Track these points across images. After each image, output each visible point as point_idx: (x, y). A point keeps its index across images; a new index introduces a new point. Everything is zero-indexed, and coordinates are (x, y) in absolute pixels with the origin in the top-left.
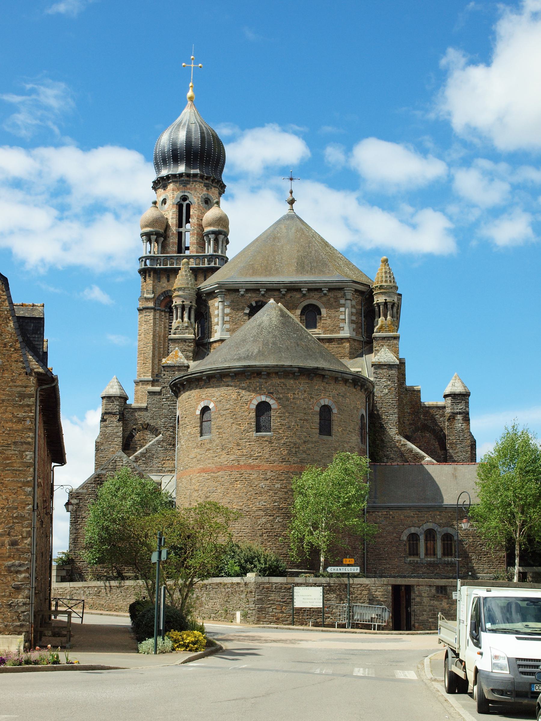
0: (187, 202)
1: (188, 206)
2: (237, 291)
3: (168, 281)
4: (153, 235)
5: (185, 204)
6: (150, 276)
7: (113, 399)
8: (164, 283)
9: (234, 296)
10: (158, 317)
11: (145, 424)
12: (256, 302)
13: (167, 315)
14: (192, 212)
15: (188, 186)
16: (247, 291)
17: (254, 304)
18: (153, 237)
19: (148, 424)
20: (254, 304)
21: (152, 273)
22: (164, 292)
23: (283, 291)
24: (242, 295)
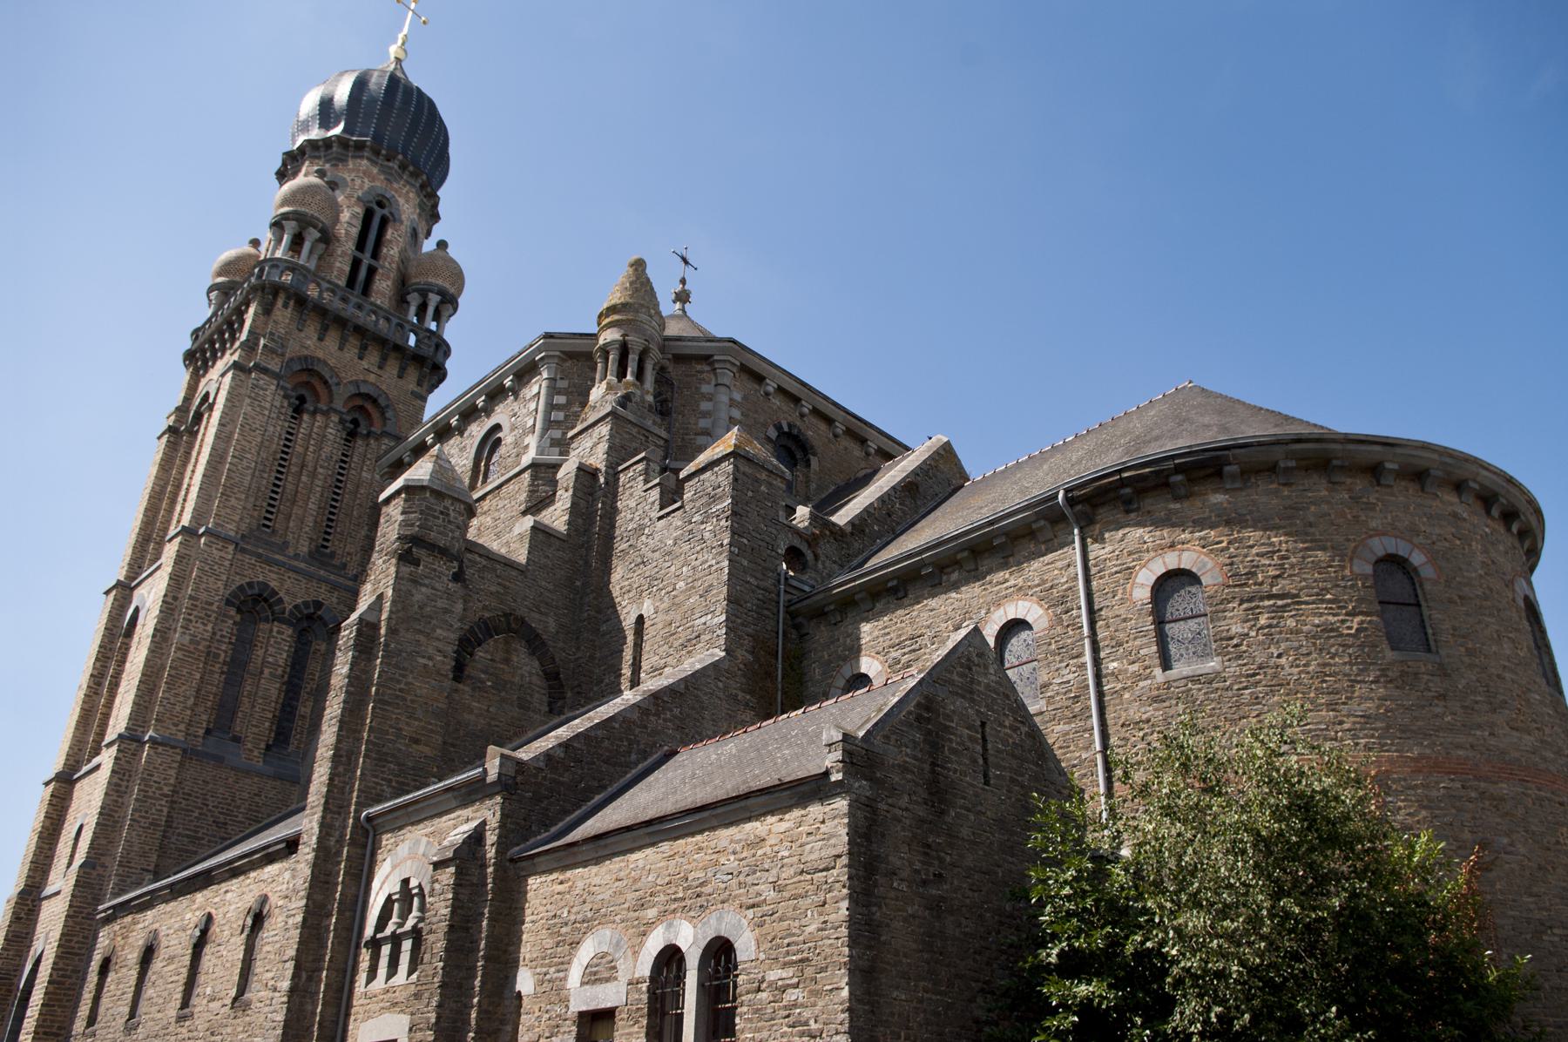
0: (386, 212)
1: (384, 222)
2: (759, 378)
3: (321, 339)
4: (315, 227)
5: (379, 213)
6: (285, 306)
7: (448, 503)
8: (309, 338)
9: (751, 385)
10: (277, 404)
11: (516, 619)
12: (790, 425)
13: (290, 412)
14: (389, 234)
15: (395, 185)
16: (781, 390)
17: (786, 429)
18: (312, 235)
19: (522, 621)
20: (786, 429)
21: (292, 303)
22: (306, 358)
23: (840, 428)
24: (767, 394)
